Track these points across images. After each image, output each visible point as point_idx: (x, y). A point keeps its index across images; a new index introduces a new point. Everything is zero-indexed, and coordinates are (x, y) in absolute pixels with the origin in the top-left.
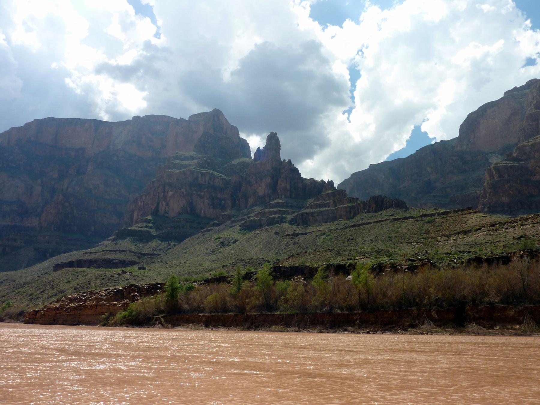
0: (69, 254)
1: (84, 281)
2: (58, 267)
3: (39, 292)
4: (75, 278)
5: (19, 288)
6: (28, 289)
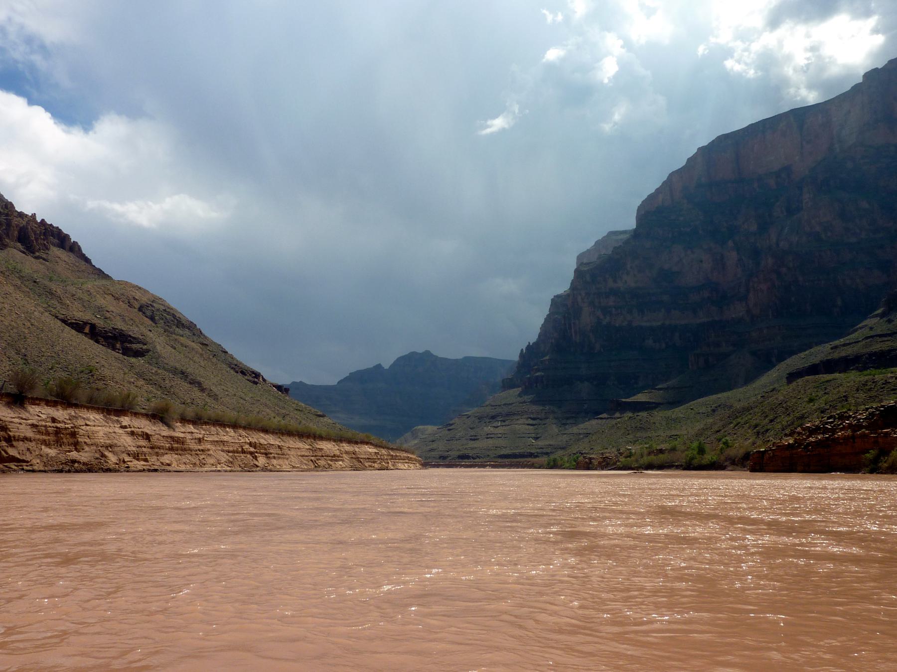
0: (807, 352)
1: (835, 397)
2: (792, 377)
3: (767, 421)
4: (821, 393)
5: (737, 417)
6: (750, 417)
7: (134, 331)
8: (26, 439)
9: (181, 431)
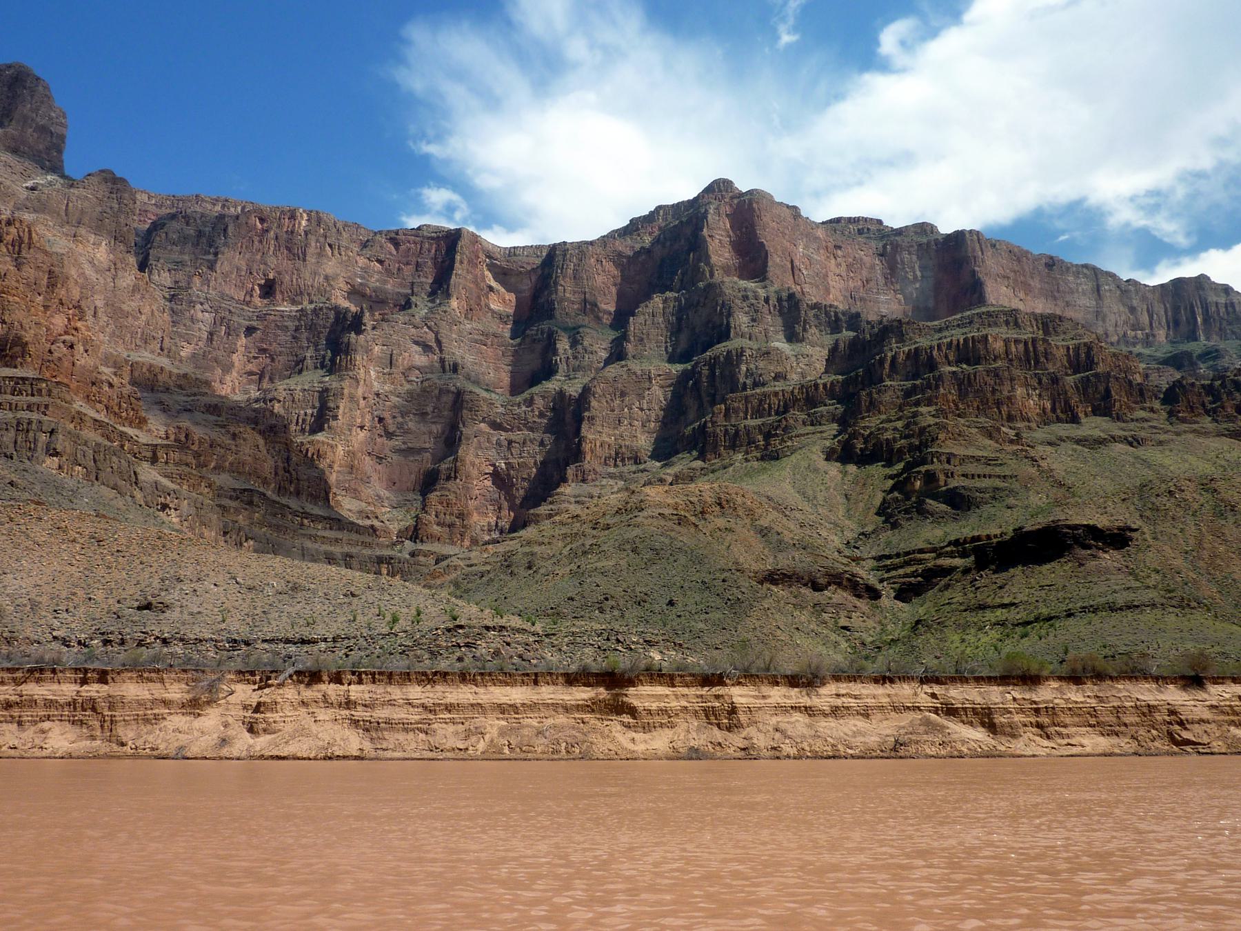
8: (1202, 721)
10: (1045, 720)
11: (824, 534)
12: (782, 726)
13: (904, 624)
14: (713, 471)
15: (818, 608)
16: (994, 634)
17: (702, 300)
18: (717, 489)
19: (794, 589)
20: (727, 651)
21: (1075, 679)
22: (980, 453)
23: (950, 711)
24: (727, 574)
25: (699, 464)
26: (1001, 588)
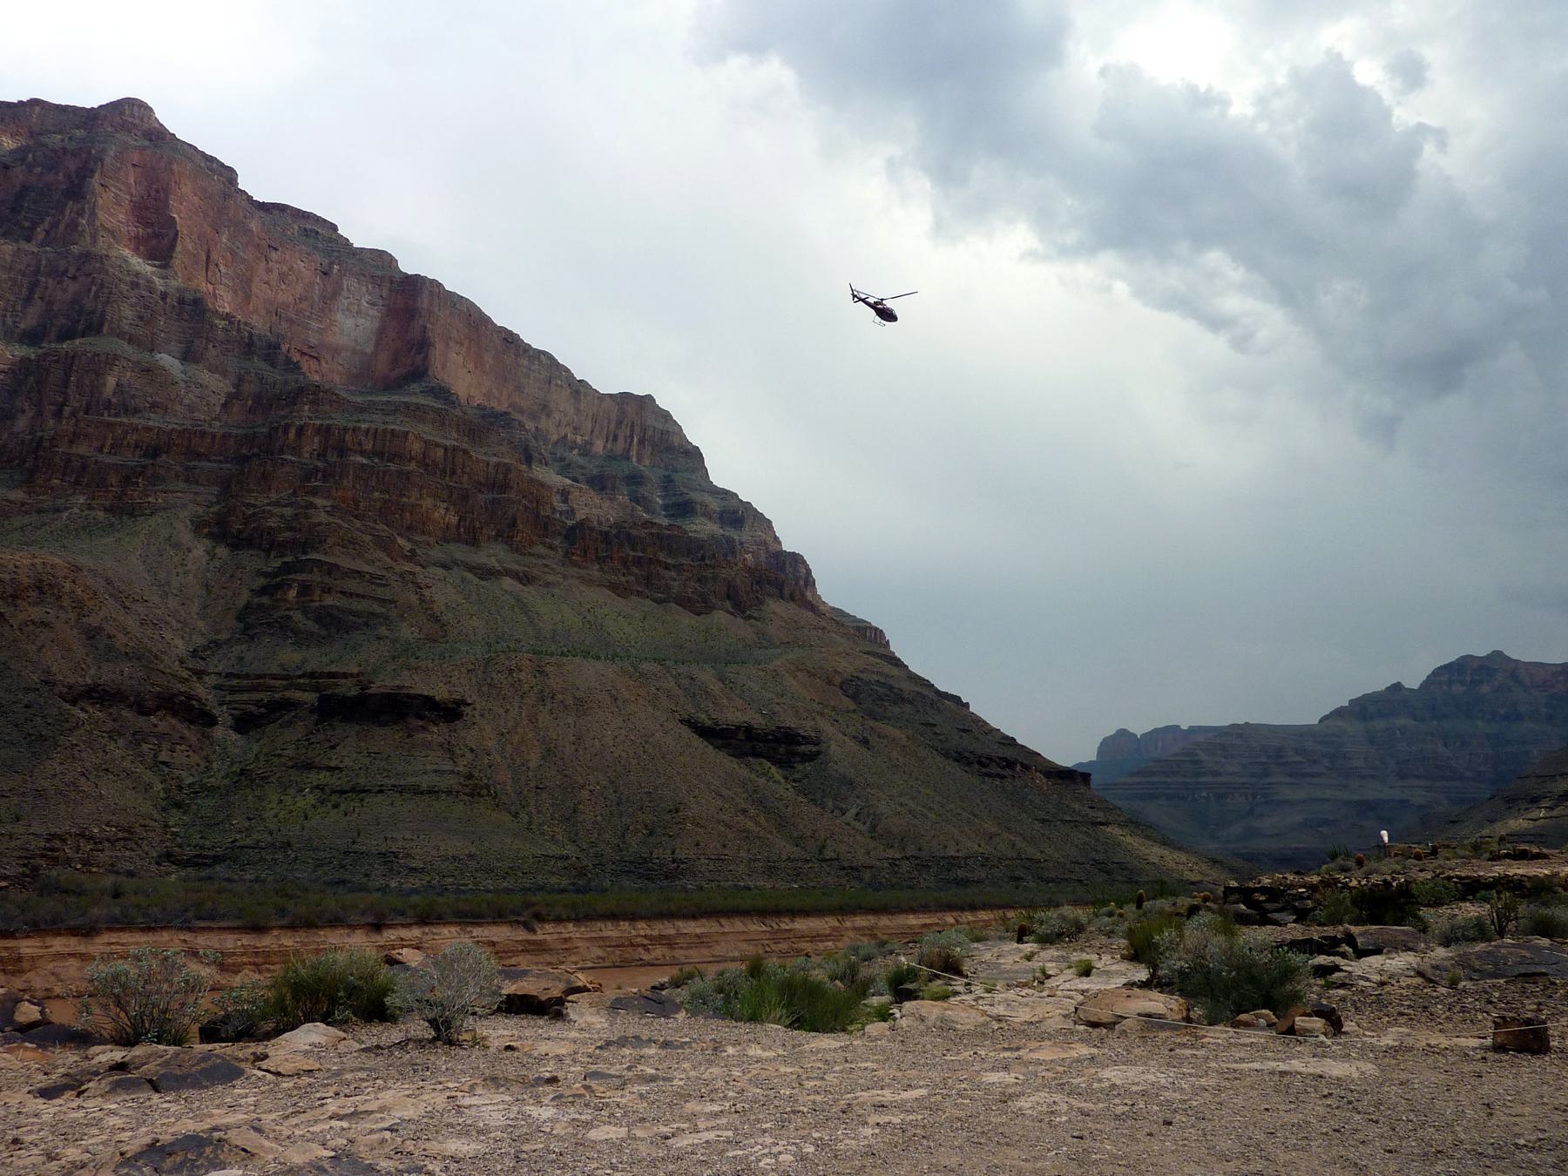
7: (806, 728)
9: (546, 933)
10: (259, 960)
11: (168, 636)
12: (58, 970)
13: (232, 763)
14: (40, 512)
15: (138, 738)
16: (311, 799)
17: (72, 271)
18: (39, 568)
19: (113, 710)
20: (16, 800)
21: (292, 927)
22: (366, 568)
23: (193, 953)
24: (31, 696)
25: (18, 495)
26: (333, 747)
